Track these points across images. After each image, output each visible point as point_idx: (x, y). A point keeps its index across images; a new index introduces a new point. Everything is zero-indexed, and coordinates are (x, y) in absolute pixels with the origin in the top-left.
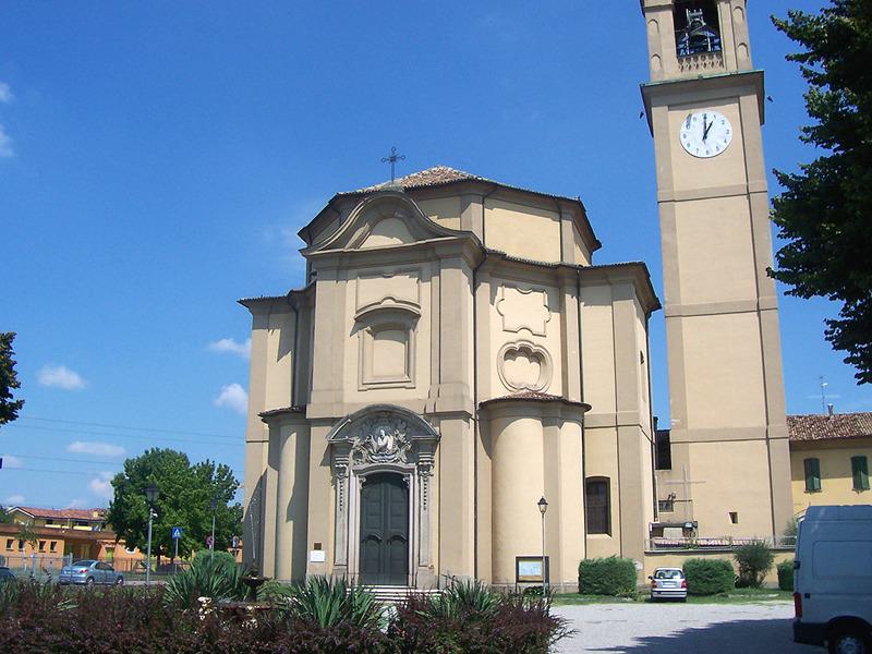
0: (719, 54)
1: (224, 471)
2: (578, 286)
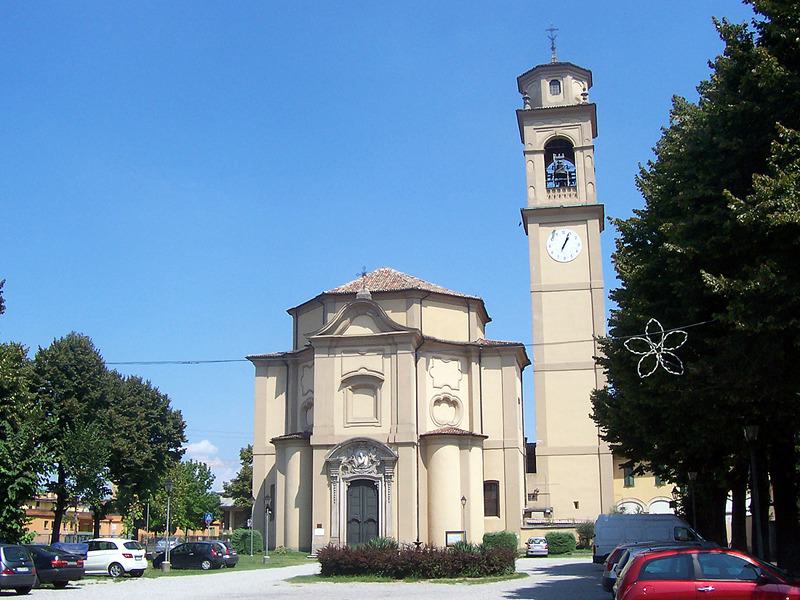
0: (575, 188)
2: (480, 357)
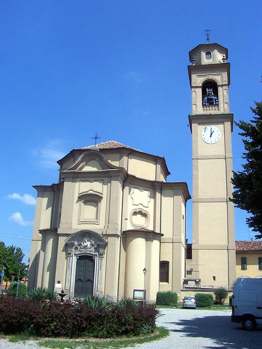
0: (218, 105)
1: (19, 250)
2: (161, 190)
